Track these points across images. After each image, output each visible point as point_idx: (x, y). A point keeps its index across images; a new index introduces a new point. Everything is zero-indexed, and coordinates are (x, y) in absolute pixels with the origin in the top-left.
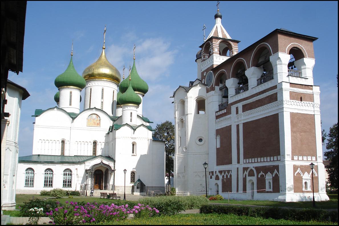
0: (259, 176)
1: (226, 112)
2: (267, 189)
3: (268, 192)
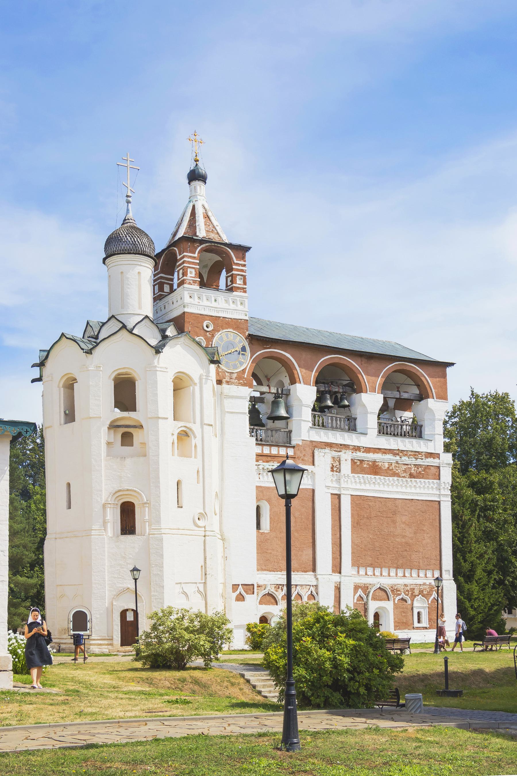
0: (396, 602)
1: (292, 454)
2: (416, 624)
3: (418, 628)
